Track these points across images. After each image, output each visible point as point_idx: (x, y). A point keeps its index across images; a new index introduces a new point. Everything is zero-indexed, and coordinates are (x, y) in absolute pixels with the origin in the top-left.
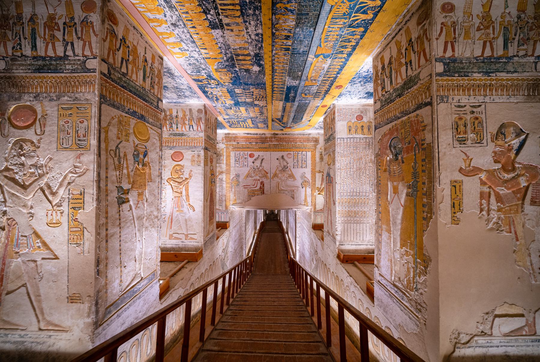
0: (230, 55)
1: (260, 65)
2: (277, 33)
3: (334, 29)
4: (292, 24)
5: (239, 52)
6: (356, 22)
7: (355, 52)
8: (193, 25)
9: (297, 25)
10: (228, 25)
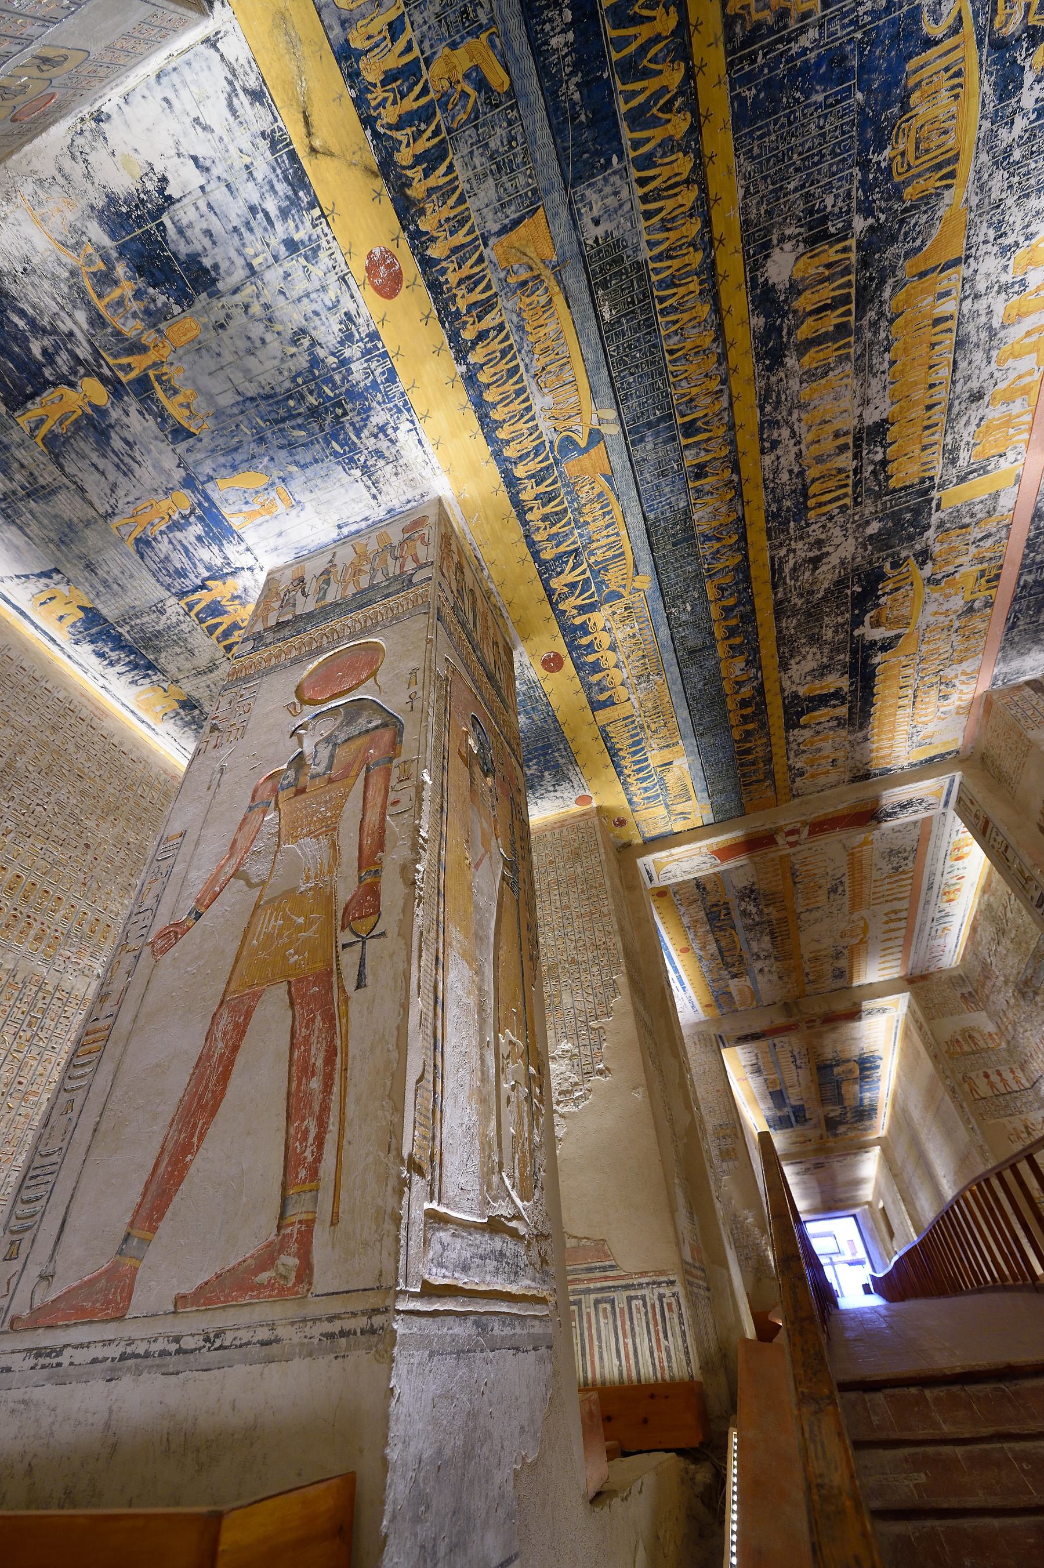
0: (865, 322)
1: (765, 299)
2: (727, 474)
3: (604, 533)
4: (700, 514)
5: (830, 352)
6: (571, 564)
7: (504, 495)
8: (929, 413)
9: (687, 512)
10: (842, 449)
